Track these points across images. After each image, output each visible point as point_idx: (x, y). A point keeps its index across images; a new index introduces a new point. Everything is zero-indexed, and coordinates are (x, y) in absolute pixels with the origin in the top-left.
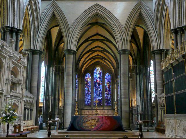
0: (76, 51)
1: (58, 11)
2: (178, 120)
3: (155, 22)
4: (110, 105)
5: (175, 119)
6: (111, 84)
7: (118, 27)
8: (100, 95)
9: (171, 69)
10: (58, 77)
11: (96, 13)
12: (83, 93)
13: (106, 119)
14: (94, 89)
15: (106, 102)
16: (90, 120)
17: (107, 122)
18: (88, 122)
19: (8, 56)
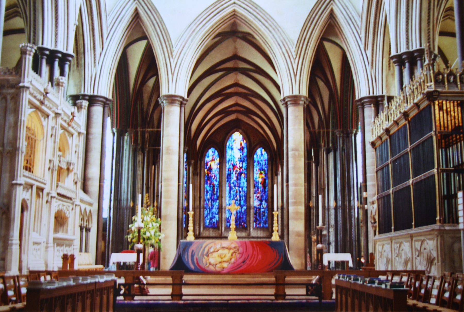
0: (186, 97)
1: (146, 7)
2: (397, 243)
3: (363, 36)
4: (267, 225)
5: (392, 242)
6: (269, 175)
7: (281, 44)
8: (242, 202)
9: (387, 140)
10: (140, 158)
11: (233, 13)
12: (200, 197)
13: (253, 247)
14: (228, 188)
15: (256, 218)
16: (218, 250)
17: (255, 253)
18: (216, 254)
19: (53, 112)
